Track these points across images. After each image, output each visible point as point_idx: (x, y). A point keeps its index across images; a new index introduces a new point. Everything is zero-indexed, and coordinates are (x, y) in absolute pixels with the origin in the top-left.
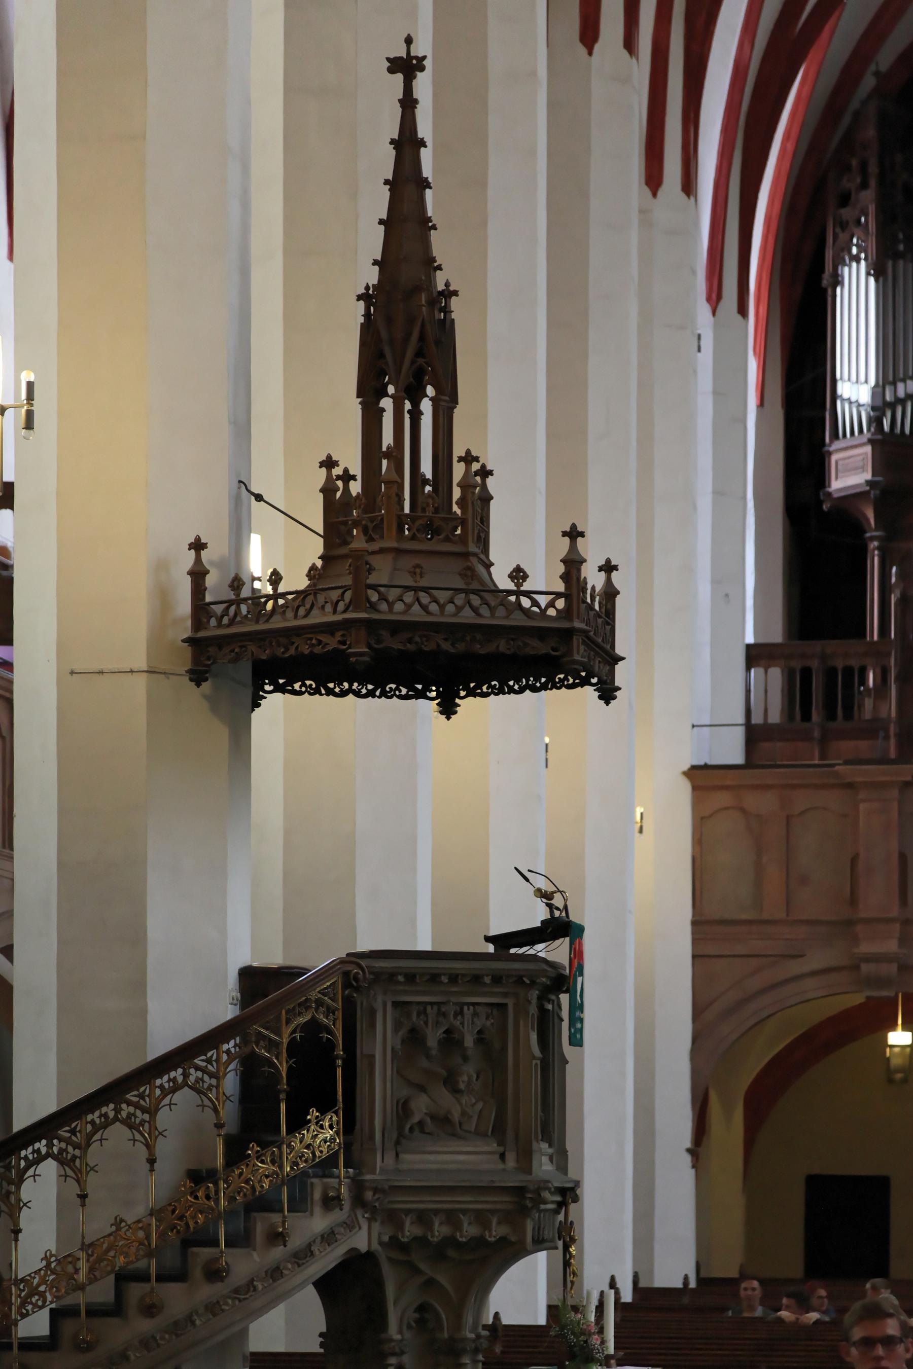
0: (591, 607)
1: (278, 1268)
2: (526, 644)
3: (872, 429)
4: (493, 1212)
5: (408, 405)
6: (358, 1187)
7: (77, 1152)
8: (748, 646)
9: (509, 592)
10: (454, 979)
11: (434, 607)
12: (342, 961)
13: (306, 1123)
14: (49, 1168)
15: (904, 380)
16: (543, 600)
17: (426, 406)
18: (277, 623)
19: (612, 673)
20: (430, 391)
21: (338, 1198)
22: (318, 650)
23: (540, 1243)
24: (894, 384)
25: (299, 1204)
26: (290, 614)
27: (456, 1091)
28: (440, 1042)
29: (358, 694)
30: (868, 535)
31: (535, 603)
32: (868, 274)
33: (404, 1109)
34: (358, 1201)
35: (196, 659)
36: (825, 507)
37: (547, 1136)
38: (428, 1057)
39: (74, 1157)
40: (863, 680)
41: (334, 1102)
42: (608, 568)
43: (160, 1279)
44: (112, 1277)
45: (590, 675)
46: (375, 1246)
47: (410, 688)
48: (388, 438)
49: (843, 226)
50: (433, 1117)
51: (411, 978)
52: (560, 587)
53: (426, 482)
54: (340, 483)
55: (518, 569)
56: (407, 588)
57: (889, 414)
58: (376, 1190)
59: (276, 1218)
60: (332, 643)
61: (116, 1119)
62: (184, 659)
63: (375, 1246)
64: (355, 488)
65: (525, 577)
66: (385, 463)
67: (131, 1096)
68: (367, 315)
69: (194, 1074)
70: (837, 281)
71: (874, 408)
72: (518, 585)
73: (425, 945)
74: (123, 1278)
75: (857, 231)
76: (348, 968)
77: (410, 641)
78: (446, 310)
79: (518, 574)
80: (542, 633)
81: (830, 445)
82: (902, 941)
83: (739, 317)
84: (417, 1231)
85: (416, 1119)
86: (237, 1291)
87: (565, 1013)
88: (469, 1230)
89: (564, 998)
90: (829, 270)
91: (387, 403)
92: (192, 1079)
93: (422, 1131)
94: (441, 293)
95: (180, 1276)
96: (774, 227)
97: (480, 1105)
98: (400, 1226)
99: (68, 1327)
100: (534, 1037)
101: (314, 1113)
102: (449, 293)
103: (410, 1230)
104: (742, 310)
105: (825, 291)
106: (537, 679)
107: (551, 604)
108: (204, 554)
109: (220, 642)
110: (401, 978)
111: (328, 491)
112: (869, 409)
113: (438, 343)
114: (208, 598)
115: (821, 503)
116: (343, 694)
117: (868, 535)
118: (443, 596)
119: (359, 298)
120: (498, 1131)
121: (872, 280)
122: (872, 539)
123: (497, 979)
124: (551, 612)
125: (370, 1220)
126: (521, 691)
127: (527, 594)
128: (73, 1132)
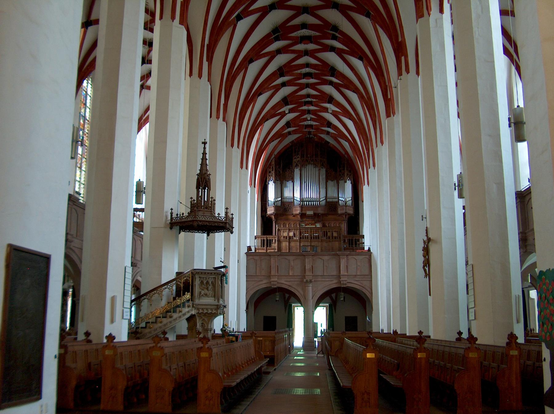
0: (230, 220)
1: (180, 316)
2: (220, 224)
4: (213, 309)
5: (203, 190)
6: (193, 304)
7: (150, 298)
9: (217, 217)
10: (208, 273)
11: (206, 218)
12: (191, 270)
13: (185, 294)
14: (146, 300)
16: (222, 218)
17: (206, 190)
18: (183, 220)
19: (233, 230)
20: (207, 188)
21: (190, 306)
22: (189, 224)
23: (220, 314)
24: (277, 199)
25: (184, 306)
26: (185, 219)
27: (208, 290)
28: (206, 283)
29: (195, 232)
31: (221, 218)
33: (200, 293)
34: (193, 307)
35: (171, 226)
36: (267, 216)
37: (222, 298)
38: (204, 285)
39: (150, 299)
40: (272, 242)
41: (190, 291)
42: (232, 214)
43: (163, 317)
44: (155, 317)
45: (229, 230)
46: (195, 313)
47: (203, 232)
48: (200, 195)
49: (270, 176)
50: (205, 294)
51: (202, 273)
52: (225, 216)
53: (206, 201)
54: (193, 201)
55: (219, 213)
56: (202, 216)
57: (276, 203)
58: (196, 305)
59: (180, 309)
60: (191, 223)
61: (156, 293)
62: (169, 226)
63: (195, 313)
64: (195, 202)
65: (220, 215)
66: (200, 198)
67: (159, 290)
68: (198, 177)
69: (168, 286)
72: (219, 216)
73: (205, 268)
74: (157, 317)
76: (192, 271)
77: (203, 223)
78: (209, 177)
79: (219, 214)
80: (222, 223)
82: (278, 279)
84: (202, 311)
85: (202, 294)
86: (174, 320)
87: (225, 280)
88: (210, 311)
89: (225, 277)
91: (200, 190)
92: (168, 287)
93: (203, 296)
94: (209, 175)
95: (166, 317)
97: (212, 293)
98: (199, 310)
99: (148, 325)
100: (220, 282)
101: (186, 293)
102: (210, 175)
103: (201, 311)
104: (255, 187)
106: (222, 230)
107: (224, 218)
108: (173, 210)
109: (175, 223)
110: (200, 273)
111: (191, 202)
113: (208, 181)
114: (173, 217)
115: (266, 215)
116: (193, 232)
118: (207, 217)
119: (197, 175)
120: (215, 296)
121: (274, 184)
123: (215, 274)
124: (224, 220)
125: (195, 309)
126: (219, 232)
127: (220, 217)
128: (150, 295)
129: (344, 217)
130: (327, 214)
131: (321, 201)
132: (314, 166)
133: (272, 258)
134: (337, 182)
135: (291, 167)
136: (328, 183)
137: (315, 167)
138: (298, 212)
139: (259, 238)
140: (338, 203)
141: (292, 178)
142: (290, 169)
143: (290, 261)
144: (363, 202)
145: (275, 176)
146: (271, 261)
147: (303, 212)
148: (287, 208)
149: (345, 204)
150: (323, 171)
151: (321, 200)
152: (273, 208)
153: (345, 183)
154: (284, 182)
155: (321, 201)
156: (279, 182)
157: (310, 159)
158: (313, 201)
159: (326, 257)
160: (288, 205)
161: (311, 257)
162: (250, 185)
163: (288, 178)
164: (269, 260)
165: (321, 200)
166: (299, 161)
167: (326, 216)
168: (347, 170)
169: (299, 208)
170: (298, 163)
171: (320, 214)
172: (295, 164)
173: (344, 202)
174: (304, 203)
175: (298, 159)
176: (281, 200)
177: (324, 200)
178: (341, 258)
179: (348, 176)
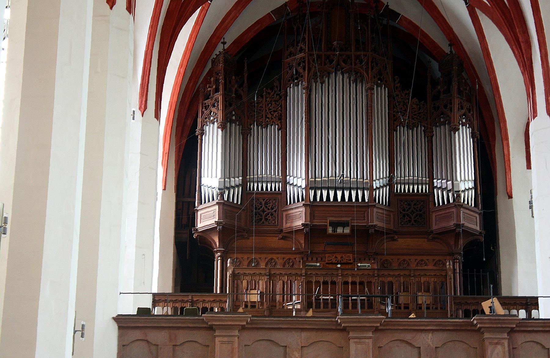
3: (219, 198)
8: (154, 295)
24: (230, 178)
32: (218, 128)
57: (227, 193)
71: (219, 189)
75: (214, 110)
81: (198, 208)
83: (155, 119)
90: (199, 128)
96: (174, 107)
104: (157, 116)
112: (217, 190)
117: (215, 250)
121: (220, 130)
122: (217, 252)
129: (452, 243)
130: (395, 233)
131: (375, 189)
132: (352, 78)
133: (217, 339)
134: (424, 131)
135: (276, 84)
137: (355, 81)
138: (299, 221)
139: (165, 301)
140: (431, 199)
141: (281, 114)
142: (272, 89)
143: (287, 349)
144: (510, 197)
145: (225, 107)
146: (213, 351)
147: (317, 222)
148: (264, 211)
149: (454, 200)
151: (375, 187)
152: (217, 207)
153: (452, 133)
155: (375, 189)
156: (236, 129)
157: (340, 55)
158: (350, 189)
159: (430, 335)
160: (266, 203)
161: (370, 334)
162: (140, 109)
163: (266, 117)
164: (208, 346)
165: (375, 187)
166: (304, 62)
167: (393, 239)
168: (460, 92)
169: (303, 209)
170: (300, 70)
171: (371, 231)
173: (450, 194)
174: (319, 193)
175: (302, 55)
176: (244, 184)
177: (385, 186)
178: (487, 343)
179: (463, 111)
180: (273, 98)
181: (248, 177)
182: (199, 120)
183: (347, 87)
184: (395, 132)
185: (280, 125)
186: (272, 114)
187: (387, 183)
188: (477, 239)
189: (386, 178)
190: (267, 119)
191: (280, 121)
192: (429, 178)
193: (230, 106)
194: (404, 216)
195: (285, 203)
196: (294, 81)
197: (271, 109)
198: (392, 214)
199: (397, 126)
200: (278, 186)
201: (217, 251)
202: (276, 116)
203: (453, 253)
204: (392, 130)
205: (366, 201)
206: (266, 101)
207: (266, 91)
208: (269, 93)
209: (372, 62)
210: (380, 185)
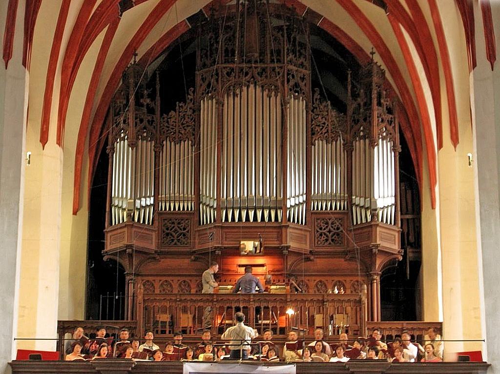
15: (145, 197)
24: (140, 199)
30: (126, 273)
36: (105, 259)
70: (113, 149)
105: (108, 155)
136: (315, 150)
142: (185, 102)
150: (297, 108)
151: (288, 206)
154: (167, 144)
156: (148, 147)
168: (379, 104)
172: (204, 86)
180: (186, 112)
181: (160, 196)
182: (110, 137)
183: (266, 99)
184: (313, 147)
185: (193, 140)
186: (185, 130)
187: (303, 201)
188: (396, 258)
189: (302, 195)
190: (180, 135)
191: (193, 136)
192: (347, 194)
193: (141, 123)
194: (321, 235)
195: (198, 223)
196: (208, 93)
197: (184, 124)
198: (308, 234)
199: (316, 140)
200: (190, 205)
201: (127, 274)
202: (189, 131)
203: (371, 275)
204: (310, 144)
205: (280, 221)
206: (179, 115)
207: (179, 105)
208: (182, 107)
209: (288, 74)
210: (299, 202)
